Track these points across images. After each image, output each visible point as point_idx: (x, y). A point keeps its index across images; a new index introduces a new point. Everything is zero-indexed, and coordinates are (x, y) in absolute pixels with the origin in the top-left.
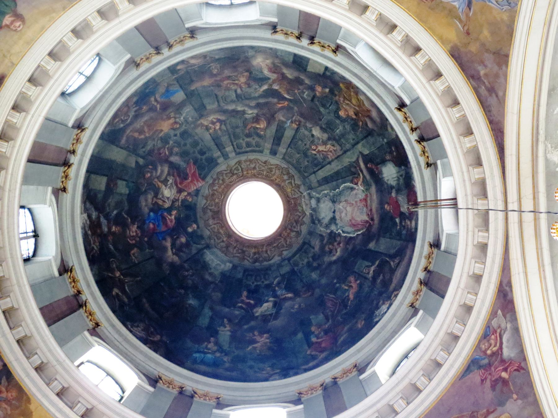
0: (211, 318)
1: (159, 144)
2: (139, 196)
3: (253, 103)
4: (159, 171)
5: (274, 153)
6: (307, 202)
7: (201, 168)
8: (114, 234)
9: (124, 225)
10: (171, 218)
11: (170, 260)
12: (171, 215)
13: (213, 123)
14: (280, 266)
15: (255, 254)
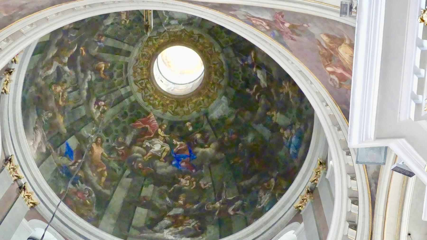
0: (265, 125)
1: (114, 155)
2: (157, 174)
3: (82, 75)
4: (138, 155)
5: (128, 54)
6: (173, 27)
7: (138, 116)
8: (185, 203)
9: (180, 191)
10: (179, 144)
11: (213, 151)
12: (177, 145)
13: (99, 107)
14: (227, 56)
15: (216, 74)
